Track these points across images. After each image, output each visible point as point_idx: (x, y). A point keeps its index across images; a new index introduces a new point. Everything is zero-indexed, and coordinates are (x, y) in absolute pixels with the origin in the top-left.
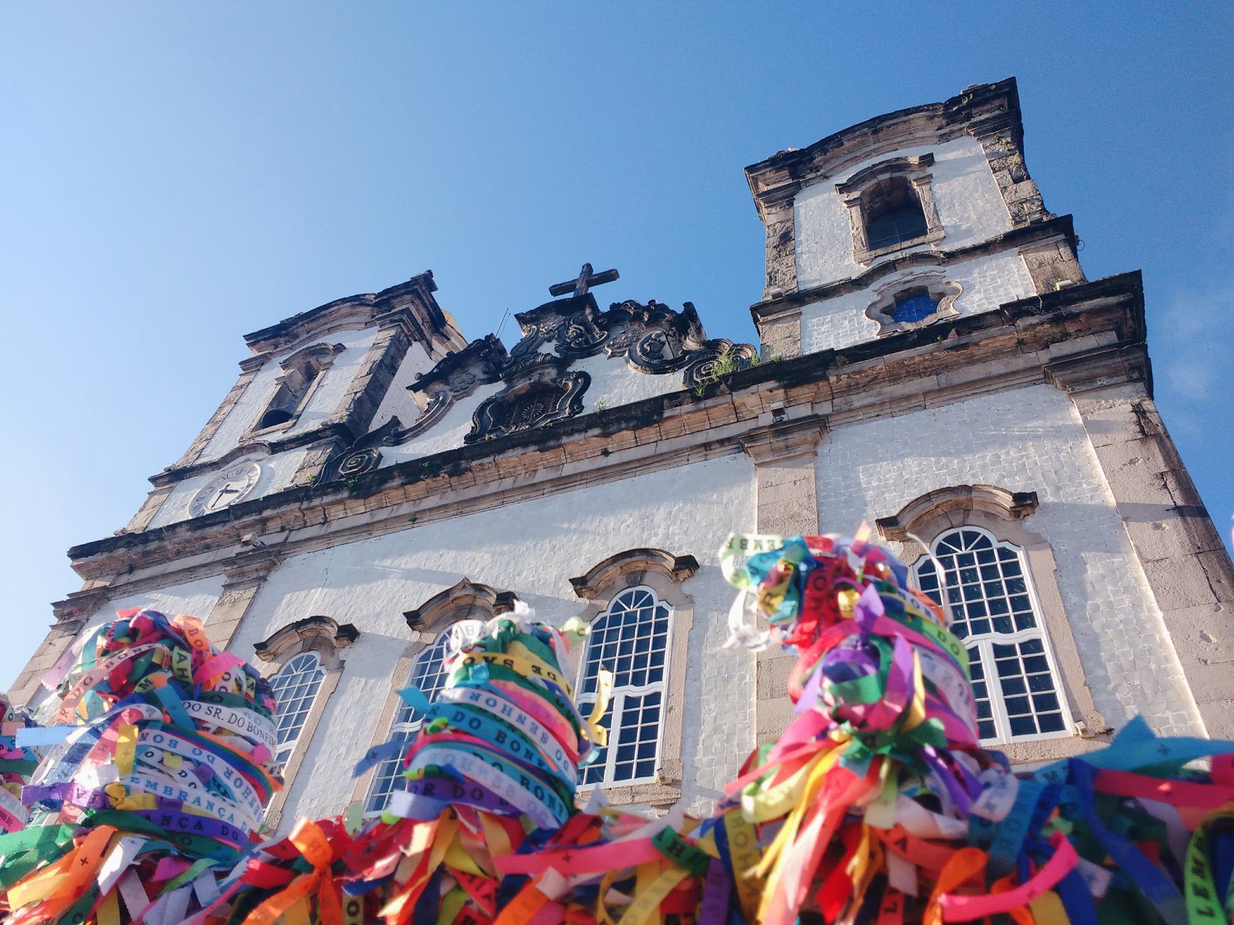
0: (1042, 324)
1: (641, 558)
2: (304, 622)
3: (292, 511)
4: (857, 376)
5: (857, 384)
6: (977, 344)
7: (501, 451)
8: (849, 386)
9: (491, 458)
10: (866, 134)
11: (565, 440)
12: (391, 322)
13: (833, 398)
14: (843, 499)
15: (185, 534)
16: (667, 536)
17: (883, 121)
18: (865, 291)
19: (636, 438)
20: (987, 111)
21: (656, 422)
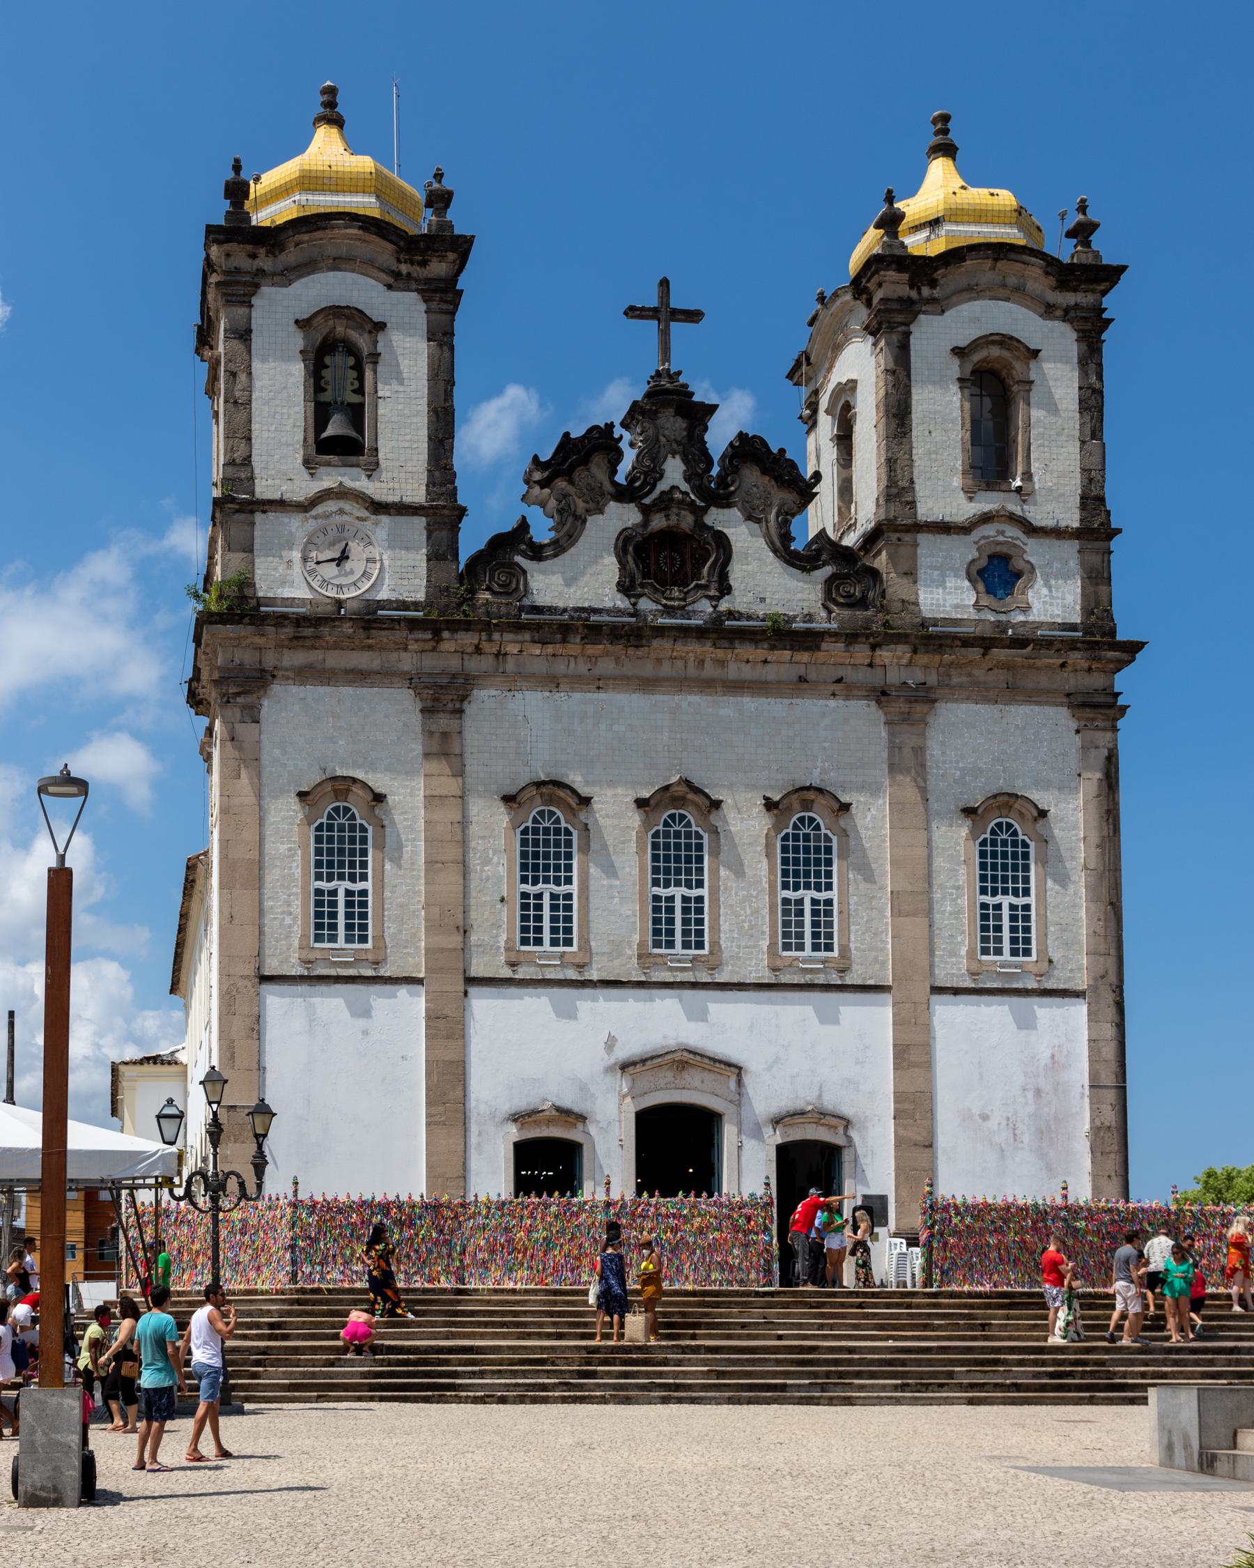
12: (442, 301)
16: (824, 771)
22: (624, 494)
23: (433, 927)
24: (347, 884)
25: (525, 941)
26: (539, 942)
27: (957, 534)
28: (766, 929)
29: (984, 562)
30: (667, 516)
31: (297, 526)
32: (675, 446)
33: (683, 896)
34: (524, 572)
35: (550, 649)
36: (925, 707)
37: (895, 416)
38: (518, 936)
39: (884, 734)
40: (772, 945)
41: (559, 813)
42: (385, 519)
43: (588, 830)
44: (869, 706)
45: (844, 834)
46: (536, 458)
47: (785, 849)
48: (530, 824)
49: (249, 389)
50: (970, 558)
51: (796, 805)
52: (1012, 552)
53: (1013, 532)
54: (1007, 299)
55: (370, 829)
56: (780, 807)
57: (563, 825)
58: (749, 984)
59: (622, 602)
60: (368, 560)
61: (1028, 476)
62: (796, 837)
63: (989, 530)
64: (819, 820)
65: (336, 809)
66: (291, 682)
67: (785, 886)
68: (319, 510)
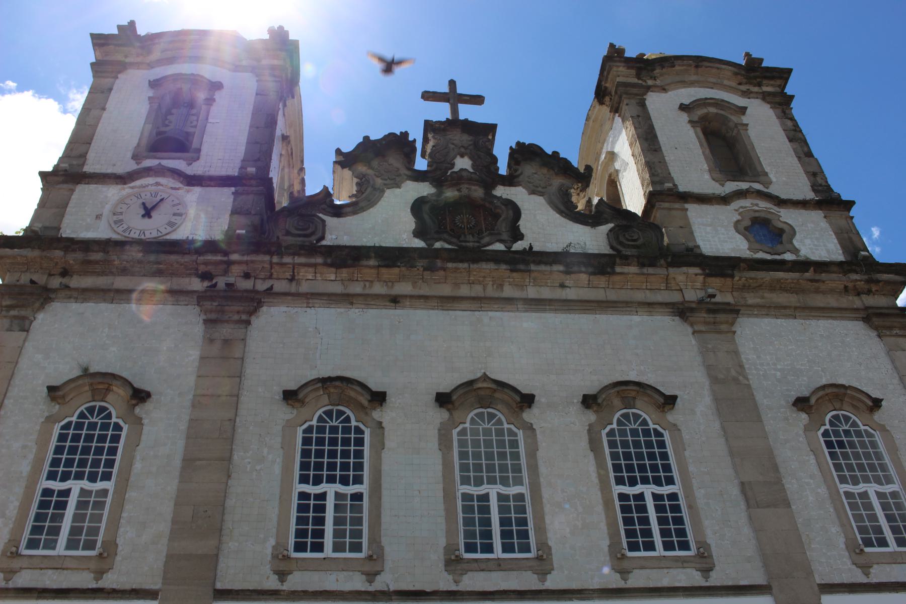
0: (860, 281)
1: (635, 388)
2: (331, 379)
3: (263, 262)
4: (751, 281)
5: (750, 286)
6: (824, 282)
7: (475, 261)
8: (744, 286)
9: (466, 265)
10: (690, 65)
11: (533, 267)
13: (732, 291)
14: (761, 373)
15: (135, 253)
17: (704, 61)
18: (728, 207)
19: (589, 280)
20: (772, 85)
21: (609, 273)
22: (420, 177)
23: (179, 528)
24: (85, 484)
25: (300, 547)
26: (319, 547)
27: (718, 204)
28: (603, 526)
29: (747, 223)
30: (459, 190)
31: (113, 192)
32: (463, 150)
33: (498, 494)
34: (323, 221)
35: (344, 273)
36: (730, 317)
37: (646, 139)
38: (292, 540)
39: (694, 342)
40: (614, 546)
41: (348, 412)
42: (197, 190)
43: (383, 428)
44: (674, 320)
45: (674, 428)
46: (338, 152)
47: (612, 444)
48: (314, 422)
49: (99, 119)
50: (735, 219)
51: (617, 402)
52: (769, 216)
53: (763, 205)
54: (712, 88)
55: (126, 428)
56: (600, 401)
57: (354, 423)
58: (594, 591)
59: (419, 243)
60: (174, 215)
61: (766, 174)
62: (623, 433)
63: (746, 203)
64: (644, 416)
65: (91, 410)
66: (72, 300)
67: (620, 481)
68: (138, 183)
